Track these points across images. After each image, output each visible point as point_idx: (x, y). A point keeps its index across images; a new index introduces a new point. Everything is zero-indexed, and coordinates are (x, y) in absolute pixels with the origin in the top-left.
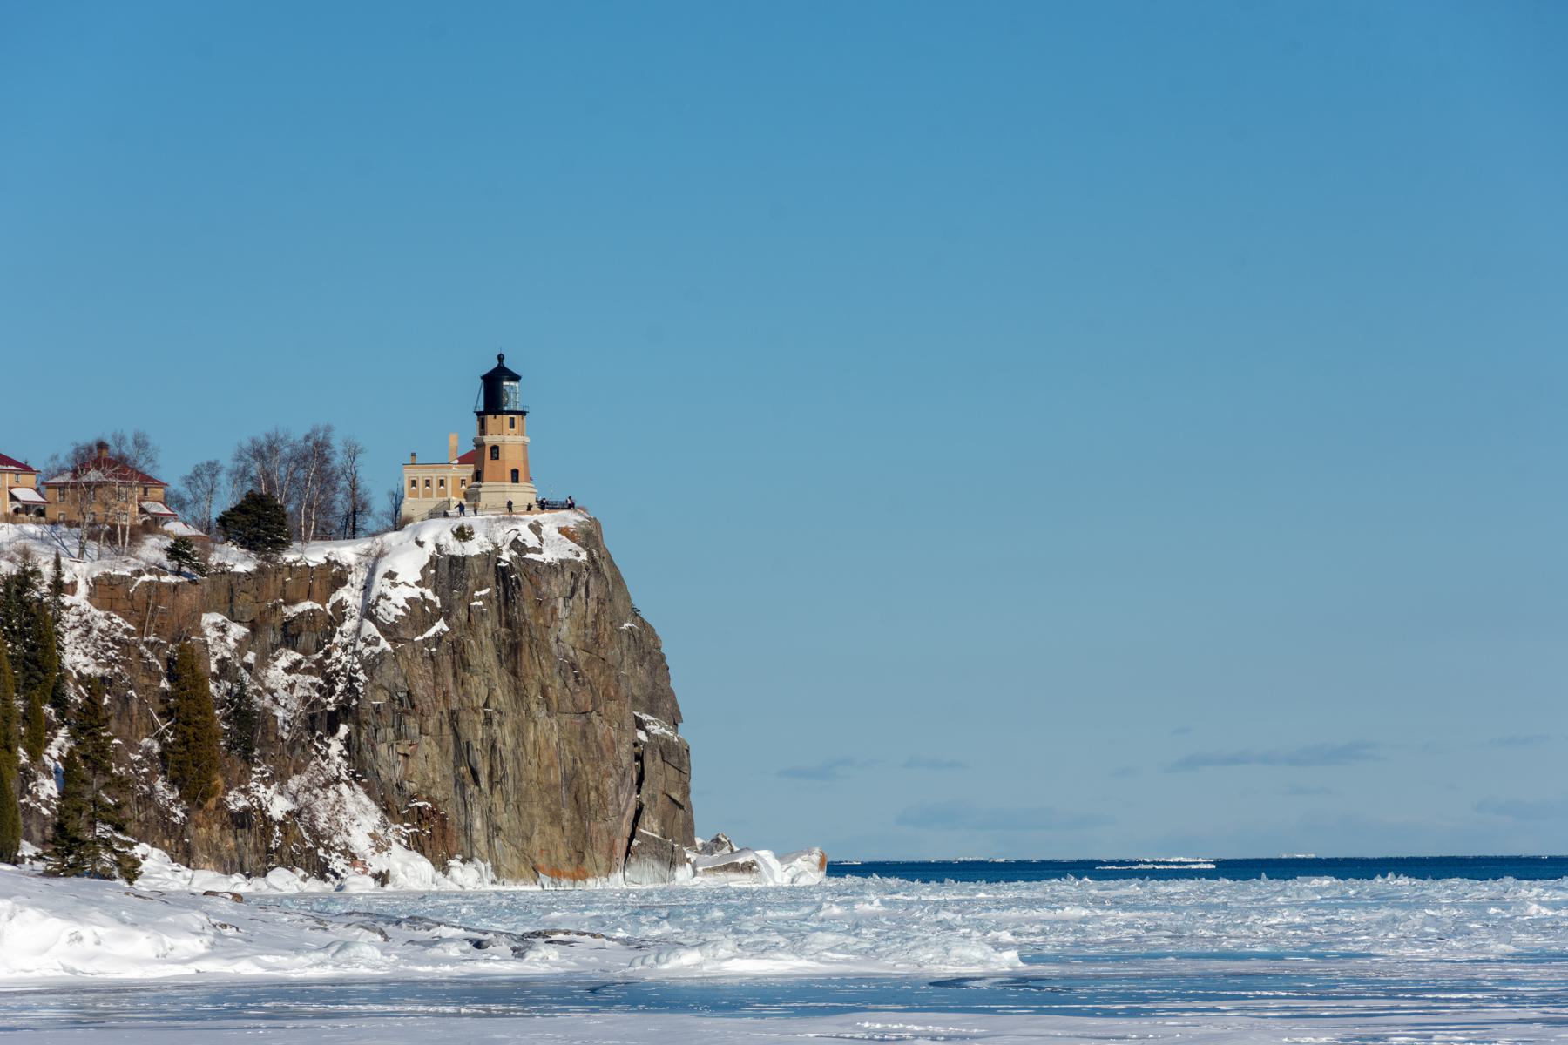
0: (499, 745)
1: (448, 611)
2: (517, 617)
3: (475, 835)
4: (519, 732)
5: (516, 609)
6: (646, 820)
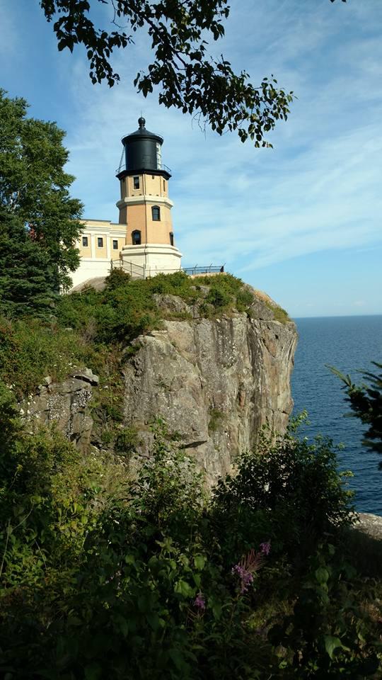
1: (220, 391)
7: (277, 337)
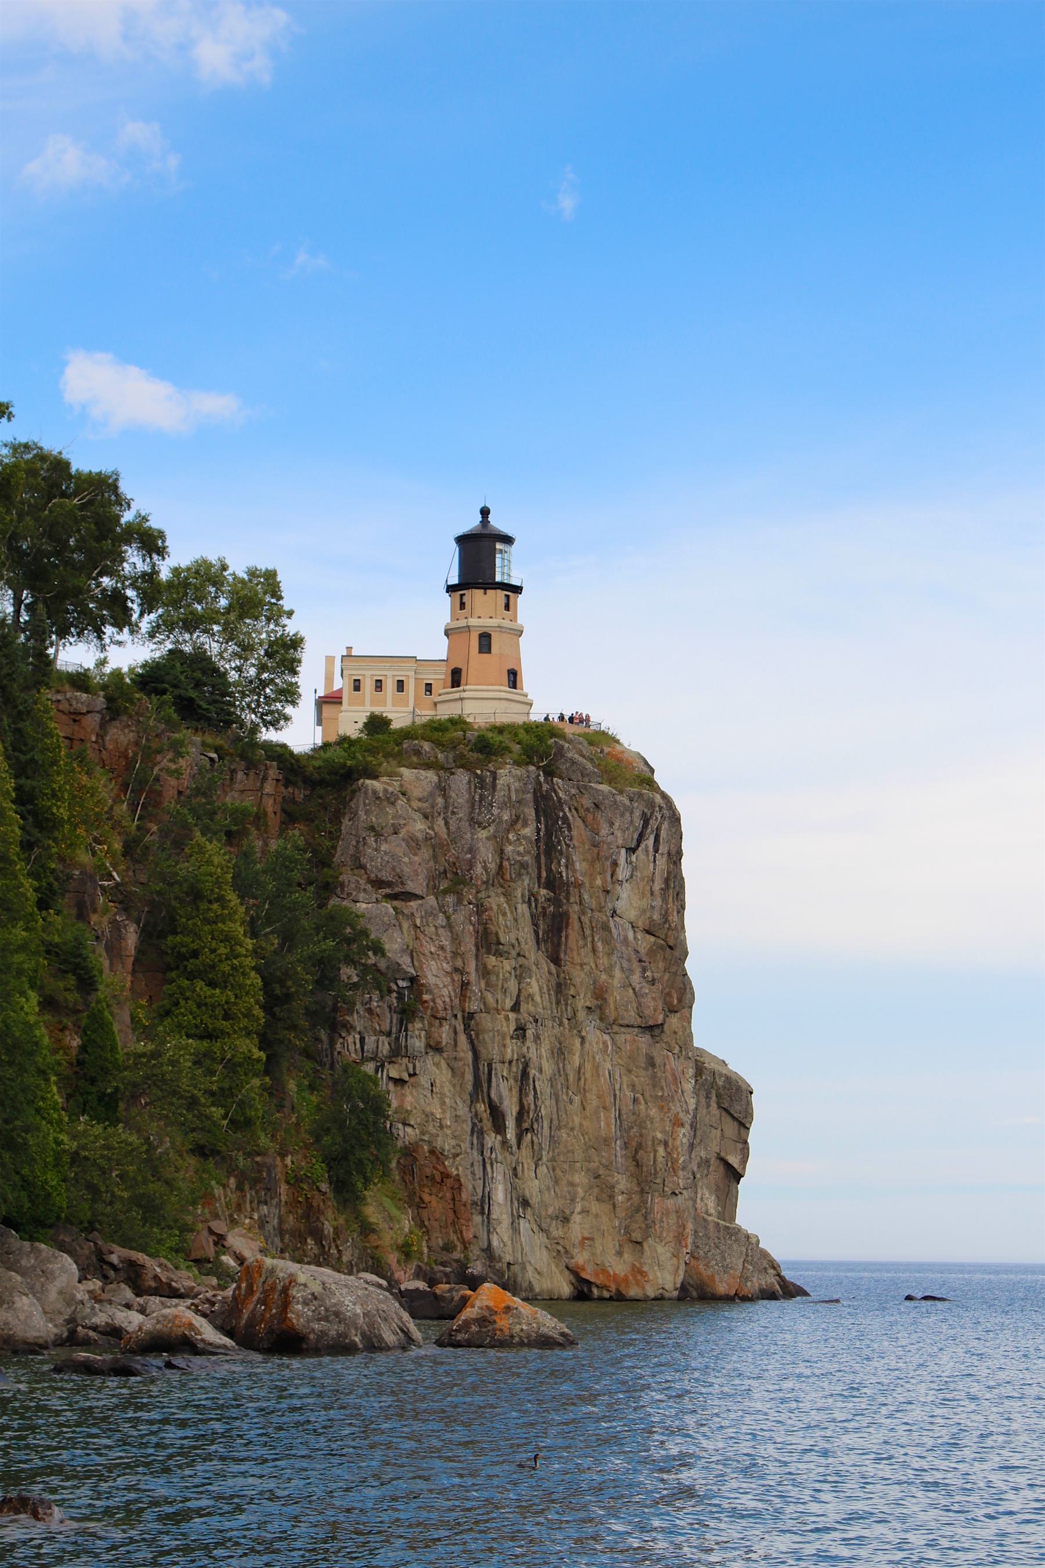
0: (533, 1072)
1: (469, 856)
2: (564, 874)
3: (494, 1216)
4: (560, 1052)
7: (597, 806)
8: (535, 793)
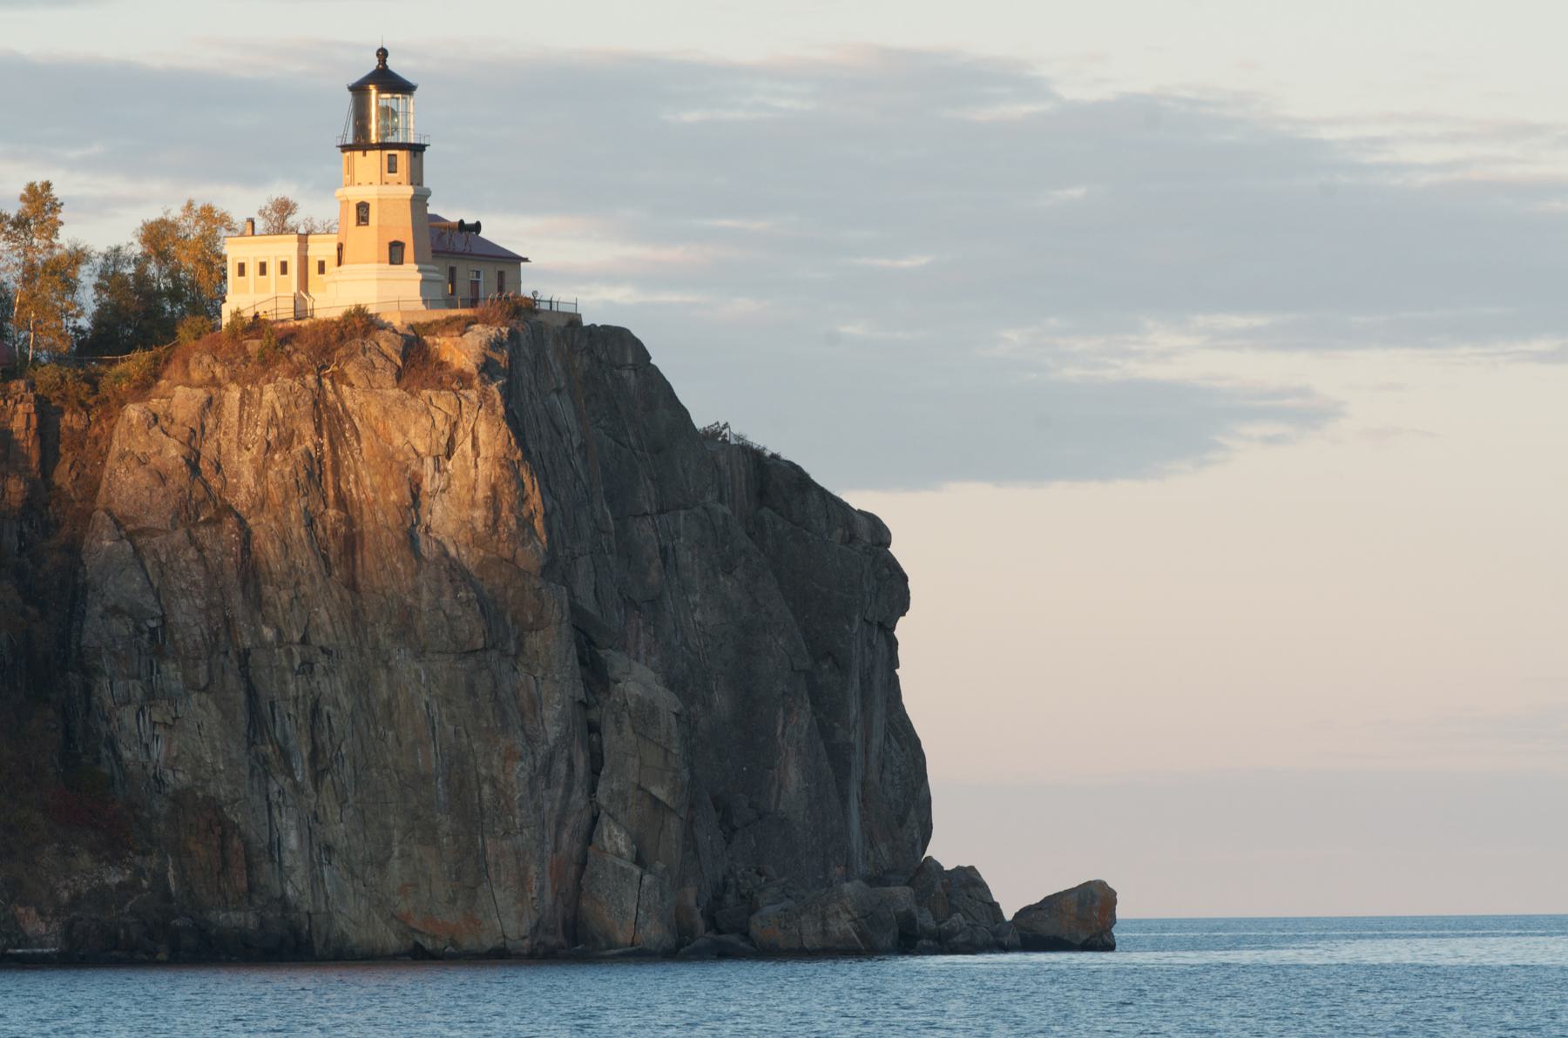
1: (235, 480)
2: (354, 491)
3: (287, 864)
4: (361, 685)
5: (352, 477)
6: (606, 833)
8: (315, 404)
